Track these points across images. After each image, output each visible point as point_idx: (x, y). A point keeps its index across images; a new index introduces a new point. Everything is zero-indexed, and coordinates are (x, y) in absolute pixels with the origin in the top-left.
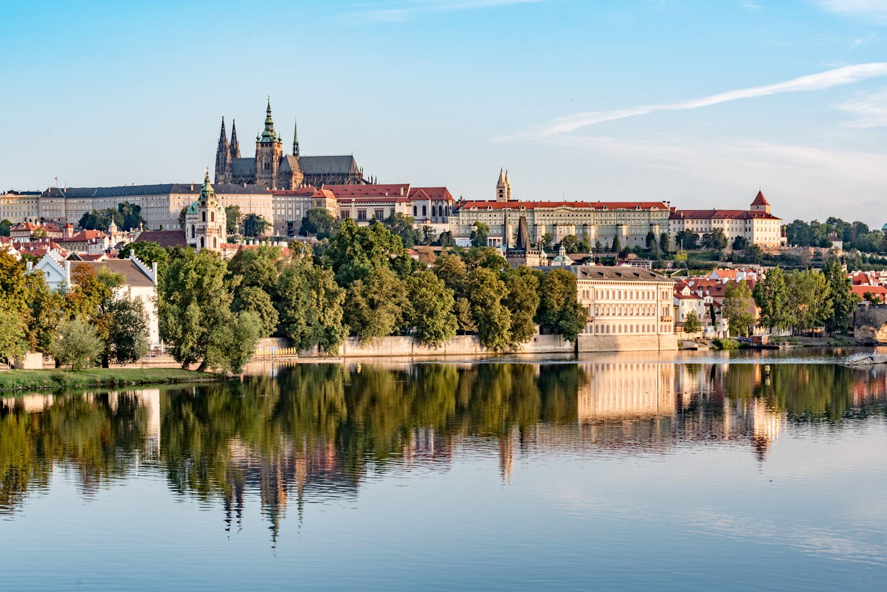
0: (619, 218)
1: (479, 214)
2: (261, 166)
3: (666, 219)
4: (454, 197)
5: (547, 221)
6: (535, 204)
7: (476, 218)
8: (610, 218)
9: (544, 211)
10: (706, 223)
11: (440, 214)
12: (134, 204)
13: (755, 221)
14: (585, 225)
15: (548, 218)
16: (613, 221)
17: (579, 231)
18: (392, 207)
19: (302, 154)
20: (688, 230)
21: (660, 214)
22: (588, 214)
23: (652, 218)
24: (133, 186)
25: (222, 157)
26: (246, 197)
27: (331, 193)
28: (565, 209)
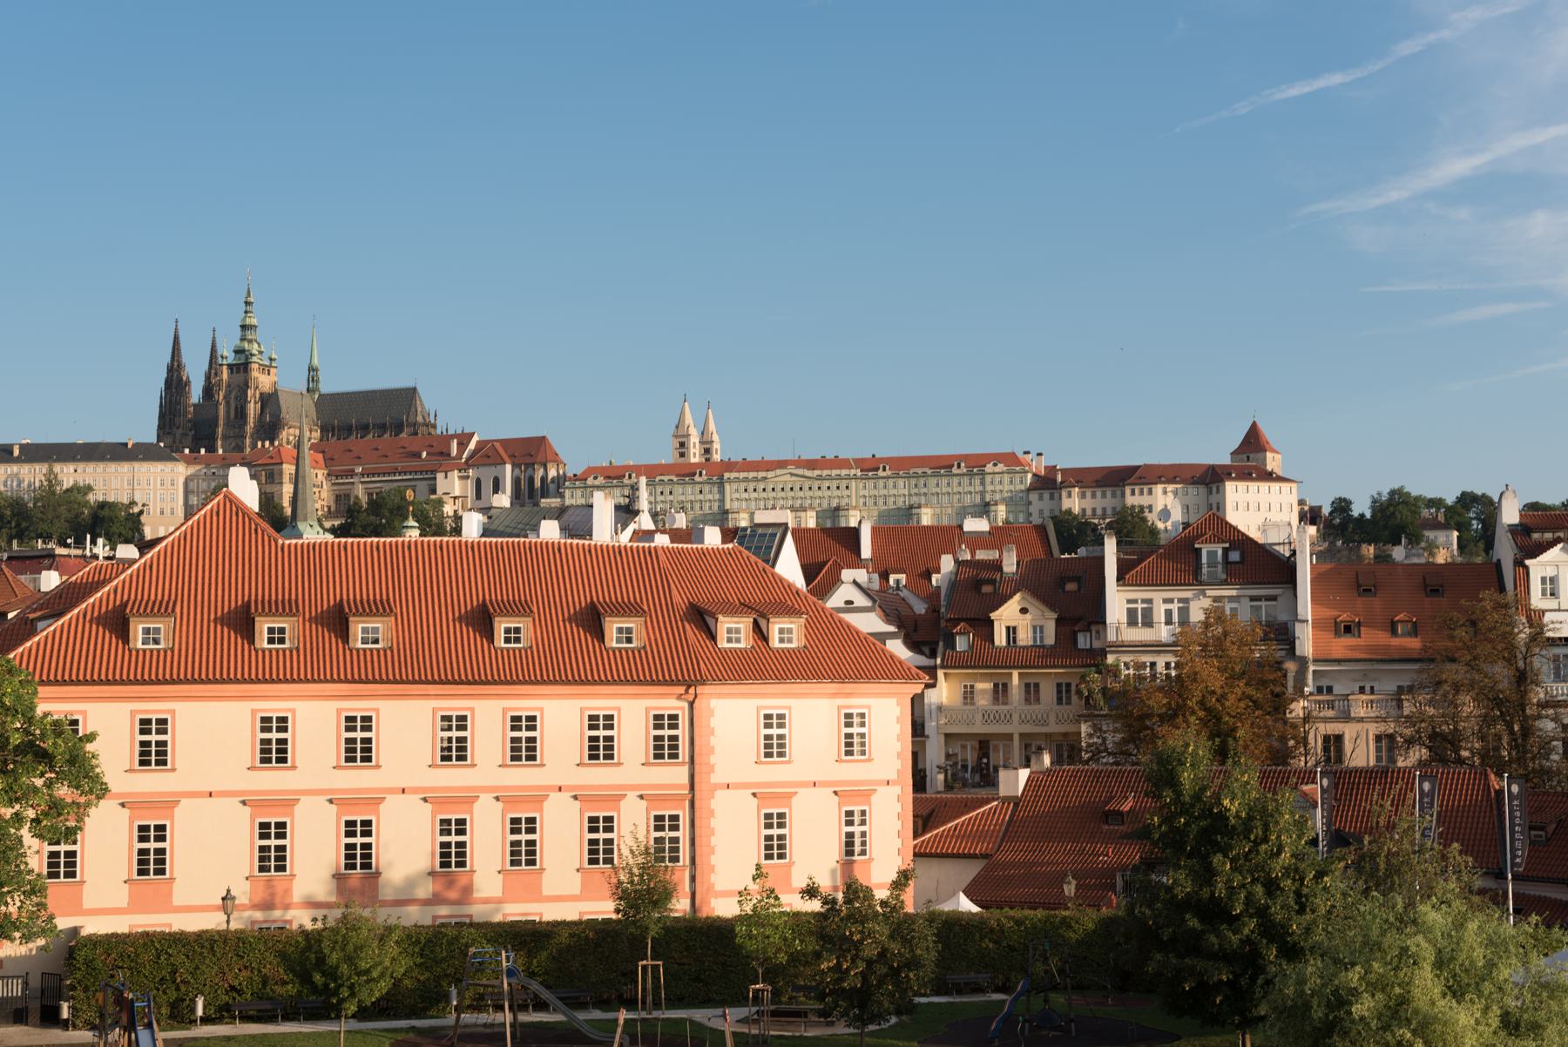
3: (1022, 491)
4: (562, 456)
6: (729, 466)
8: (895, 492)
9: (746, 480)
10: (1114, 496)
14: (837, 509)
15: (755, 495)
18: (430, 482)
19: (328, 386)
20: (1069, 512)
21: (1006, 478)
22: (843, 484)
23: (989, 488)
25: (170, 401)
26: (125, 468)
27: (321, 455)
28: (792, 474)
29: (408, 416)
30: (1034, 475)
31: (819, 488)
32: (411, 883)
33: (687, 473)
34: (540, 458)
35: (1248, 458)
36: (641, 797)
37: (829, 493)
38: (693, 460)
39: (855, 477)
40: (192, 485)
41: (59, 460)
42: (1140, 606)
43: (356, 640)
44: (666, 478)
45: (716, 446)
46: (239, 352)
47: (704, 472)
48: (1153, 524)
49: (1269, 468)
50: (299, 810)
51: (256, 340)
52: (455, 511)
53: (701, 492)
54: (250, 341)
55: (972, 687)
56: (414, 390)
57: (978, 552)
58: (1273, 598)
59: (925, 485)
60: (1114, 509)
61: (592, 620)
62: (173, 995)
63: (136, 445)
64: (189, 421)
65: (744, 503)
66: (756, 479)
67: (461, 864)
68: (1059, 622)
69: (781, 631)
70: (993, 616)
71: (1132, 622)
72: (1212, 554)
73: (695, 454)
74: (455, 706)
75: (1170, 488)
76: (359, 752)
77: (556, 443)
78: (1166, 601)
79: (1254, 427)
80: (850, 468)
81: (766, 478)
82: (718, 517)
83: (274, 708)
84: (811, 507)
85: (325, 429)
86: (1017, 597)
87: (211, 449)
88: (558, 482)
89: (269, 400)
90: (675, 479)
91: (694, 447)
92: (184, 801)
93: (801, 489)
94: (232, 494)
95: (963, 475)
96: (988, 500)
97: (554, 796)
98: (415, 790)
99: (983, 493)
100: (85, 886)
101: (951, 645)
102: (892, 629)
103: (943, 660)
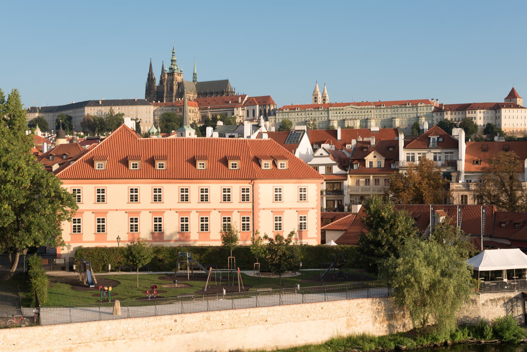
1: (290, 114)
3: (430, 113)
4: (275, 102)
5: (339, 117)
6: (331, 105)
7: (287, 117)
8: (387, 113)
9: (336, 109)
10: (462, 114)
12: (67, 115)
13: (503, 110)
14: (367, 119)
15: (339, 115)
16: (389, 116)
17: (363, 124)
19: (199, 80)
20: (447, 119)
21: (425, 108)
22: (369, 111)
23: (419, 111)
24: (73, 104)
26: (134, 108)
27: (197, 103)
28: (352, 108)
29: (225, 89)
30: (435, 107)
31: (361, 112)
32: (172, 235)
33: (316, 108)
34: (268, 103)
35: (511, 100)
36: (238, 212)
37: (364, 114)
38: (319, 103)
39: (373, 108)
40: (156, 113)
41: (114, 105)
42: (411, 155)
43: (157, 167)
44: (310, 109)
45: (327, 98)
46: (170, 69)
47: (322, 107)
48: (476, 123)
49: (518, 104)
50: (141, 214)
51: (176, 65)
52: (240, 121)
53: (321, 114)
54: (174, 65)
55: (359, 180)
56: (228, 80)
57: (364, 138)
58: (452, 153)
59: (397, 111)
60: (462, 118)
61: (225, 161)
62: (103, 264)
63: (138, 100)
64: (155, 92)
65: (336, 117)
66: (340, 109)
67: (187, 230)
68: (386, 160)
69: (281, 164)
70: (365, 158)
71: (408, 160)
72: (434, 139)
73: (320, 101)
74: (185, 186)
75: (482, 111)
76: (157, 198)
77: (273, 98)
78: (419, 154)
79: (513, 89)
80: (372, 105)
81: (343, 109)
82: (327, 122)
83: (134, 186)
84: (358, 119)
85: (198, 94)
86: (373, 152)
87: (162, 101)
88: (274, 111)
89: (181, 85)
90: (313, 110)
91: (320, 98)
93: (355, 112)
94: (125, 125)
95: (410, 107)
96: (419, 115)
97: (213, 211)
98: (174, 209)
99: (417, 113)
100: (83, 235)
101: (352, 167)
102: (334, 162)
103: (349, 172)
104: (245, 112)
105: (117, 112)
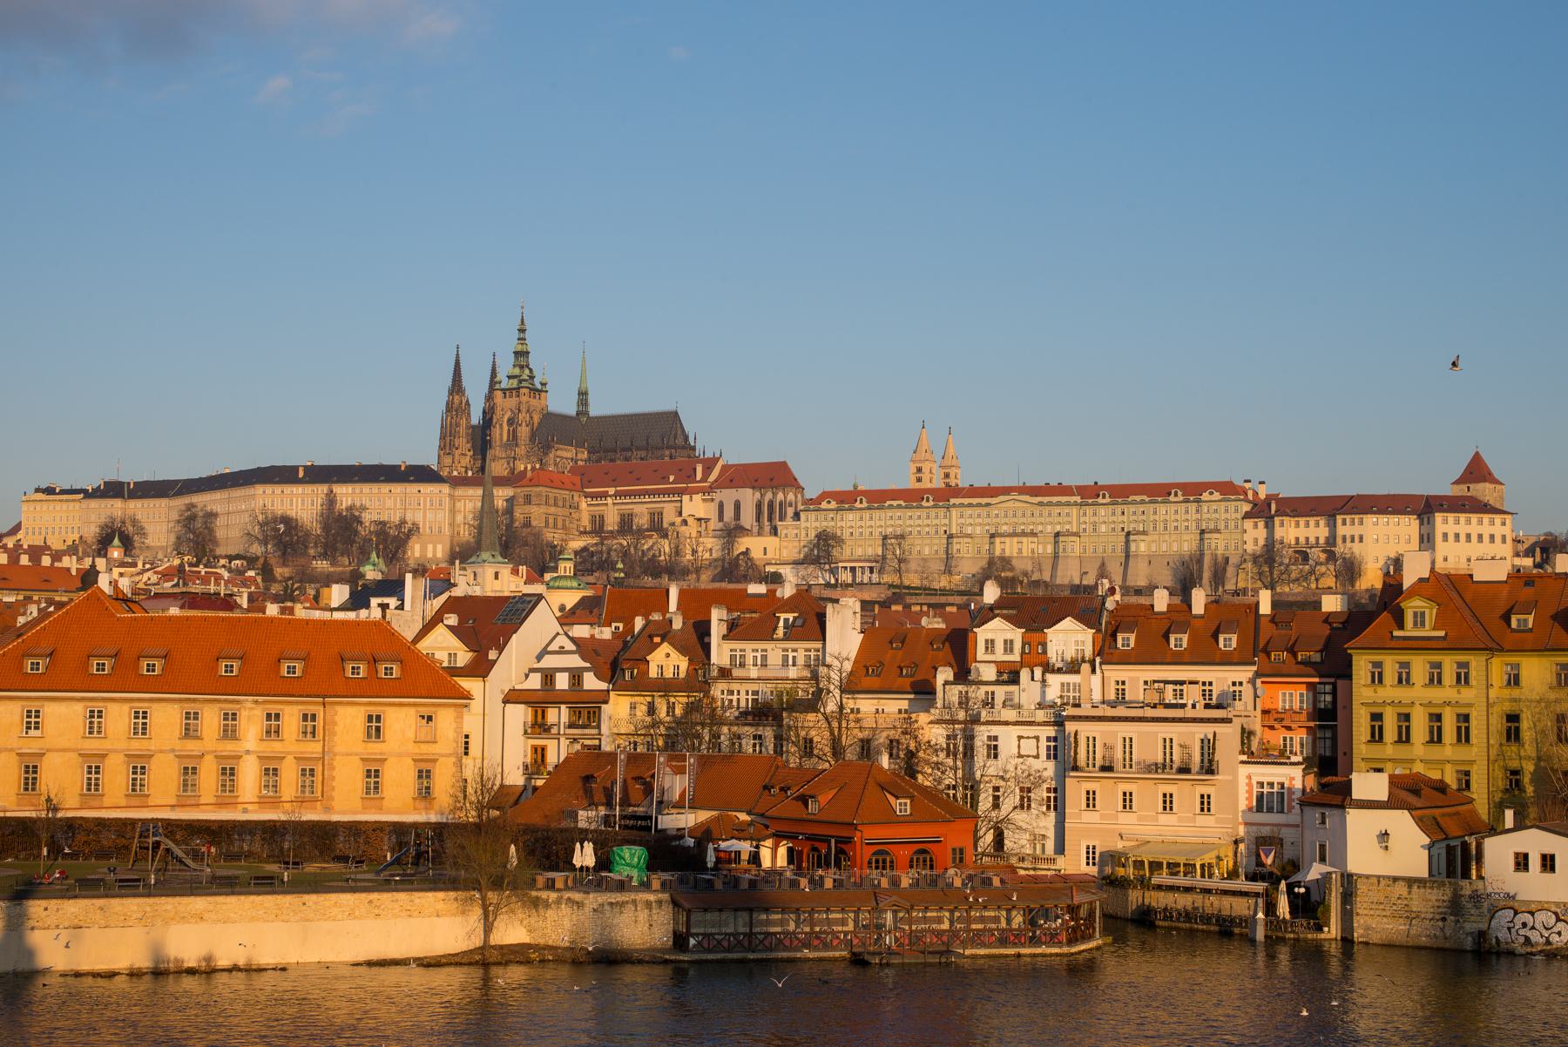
0: (1132, 518)
2: (501, 435)
7: (832, 524)
11: (770, 518)
19: (595, 410)
26: (397, 488)
35: (1468, 488)
39: (1076, 504)
42: (738, 654)
44: (895, 503)
51: (527, 366)
72: (786, 620)
78: (753, 651)
81: (988, 505)
90: (904, 504)
92: (49, 755)
94: (99, 588)
96: (1204, 528)
102: (588, 665)
104: (713, 507)
105: (347, 500)
